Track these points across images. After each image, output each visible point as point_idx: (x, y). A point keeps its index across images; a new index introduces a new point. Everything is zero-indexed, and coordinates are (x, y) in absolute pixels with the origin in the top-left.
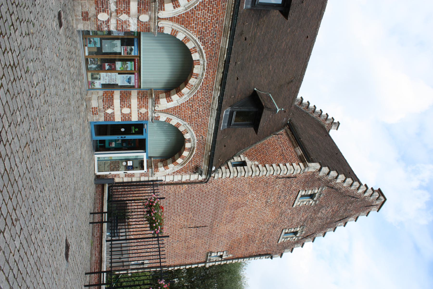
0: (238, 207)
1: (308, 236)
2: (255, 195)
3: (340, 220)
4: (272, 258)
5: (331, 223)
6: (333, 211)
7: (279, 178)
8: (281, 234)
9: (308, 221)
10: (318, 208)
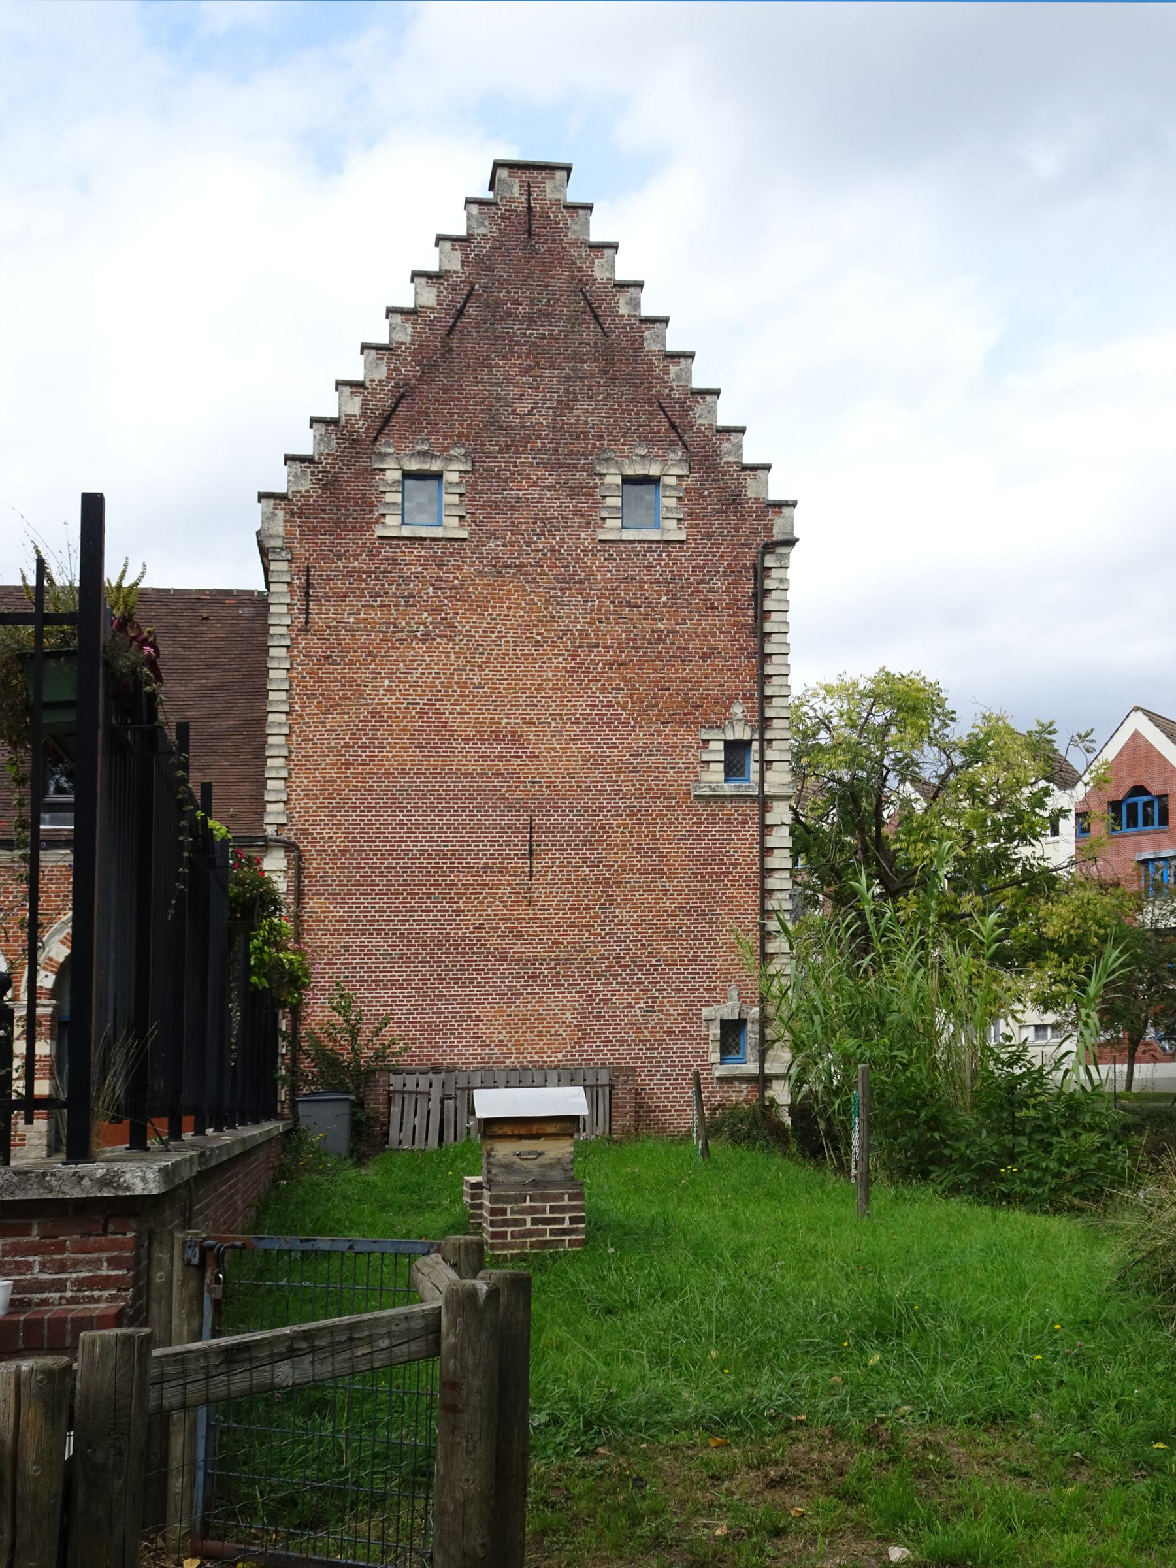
0: (444, 731)
1: (673, 426)
2: (387, 683)
3: (596, 317)
4: (791, 542)
5: (607, 354)
6: (522, 373)
7: (307, 622)
8: (631, 542)
9: (571, 453)
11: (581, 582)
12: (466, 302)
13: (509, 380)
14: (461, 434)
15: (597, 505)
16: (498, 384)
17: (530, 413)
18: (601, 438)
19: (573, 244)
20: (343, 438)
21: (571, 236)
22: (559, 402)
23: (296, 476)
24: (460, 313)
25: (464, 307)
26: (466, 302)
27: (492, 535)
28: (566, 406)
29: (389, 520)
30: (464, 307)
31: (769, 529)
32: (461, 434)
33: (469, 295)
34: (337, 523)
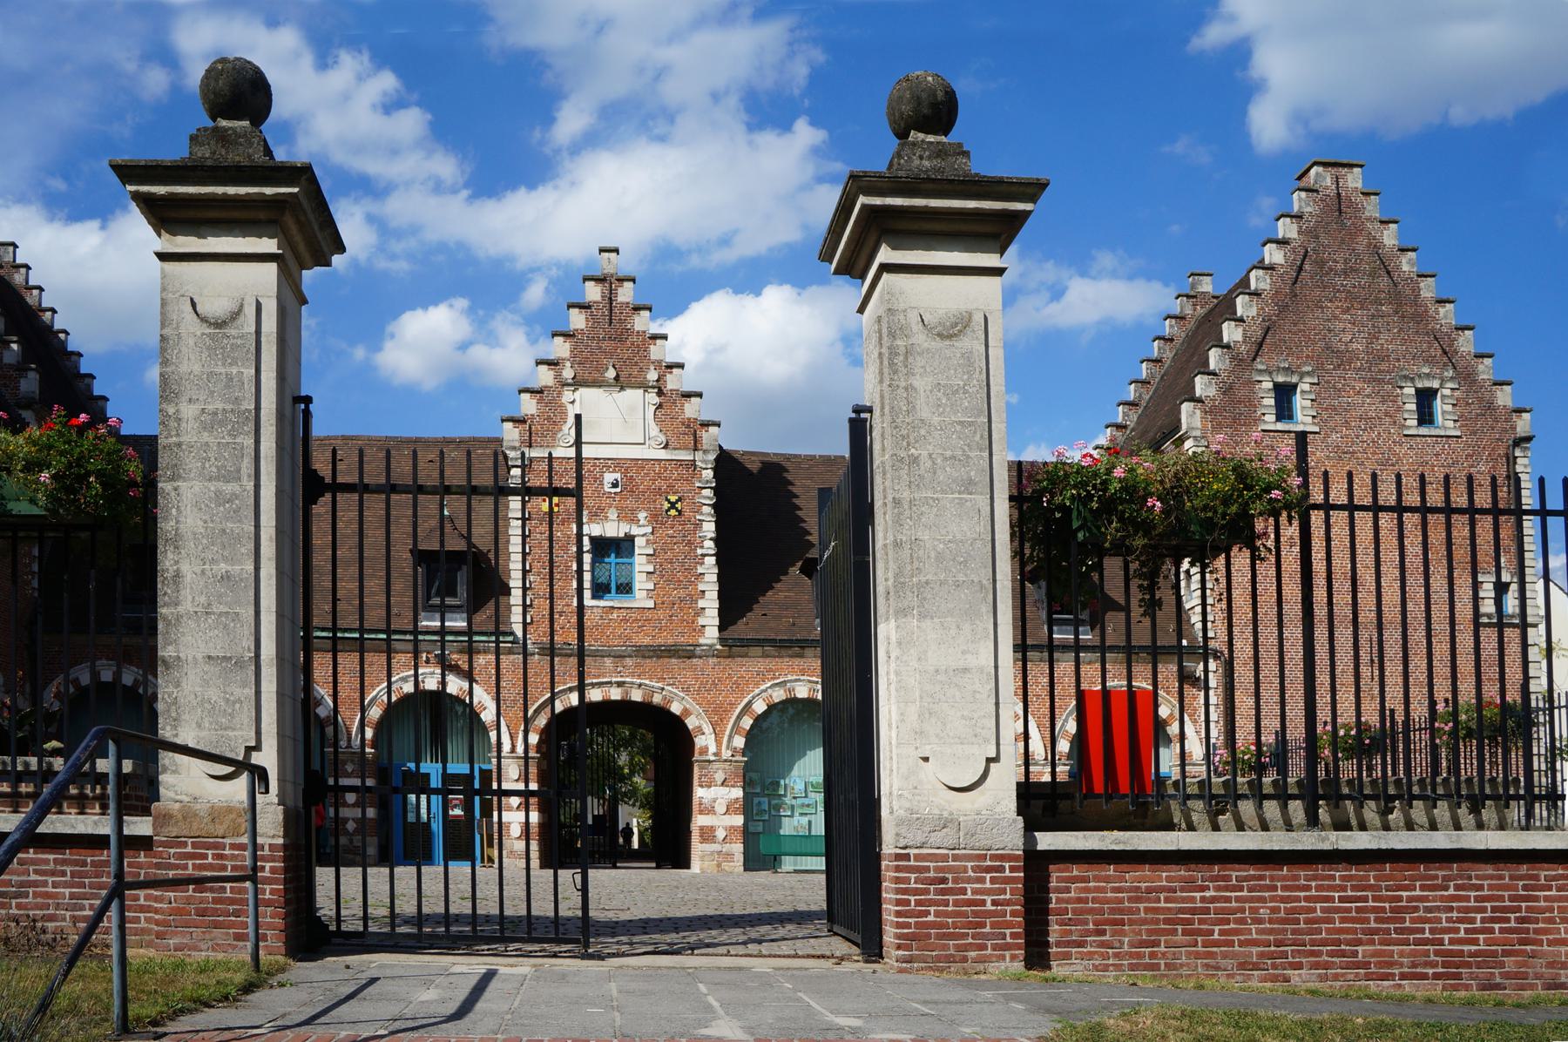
1: (1445, 352)
9: (1380, 371)
10: (1333, 359)
11: (1393, 465)
12: (1303, 261)
13: (1336, 318)
14: (1308, 356)
15: (1399, 409)
16: (1329, 320)
17: (1351, 341)
18: (1398, 360)
19: (1368, 219)
20: (1233, 358)
21: (1367, 214)
22: (1369, 334)
23: (1205, 384)
24: (1300, 269)
25: (1302, 263)
26: (1303, 261)
27: (1333, 430)
28: (1374, 337)
29: (1267, 418)
30: (1302, 263)
31: (1514, 428)
32: (1308, 356)
33: (1305, 256)
34: (1234, 419)
